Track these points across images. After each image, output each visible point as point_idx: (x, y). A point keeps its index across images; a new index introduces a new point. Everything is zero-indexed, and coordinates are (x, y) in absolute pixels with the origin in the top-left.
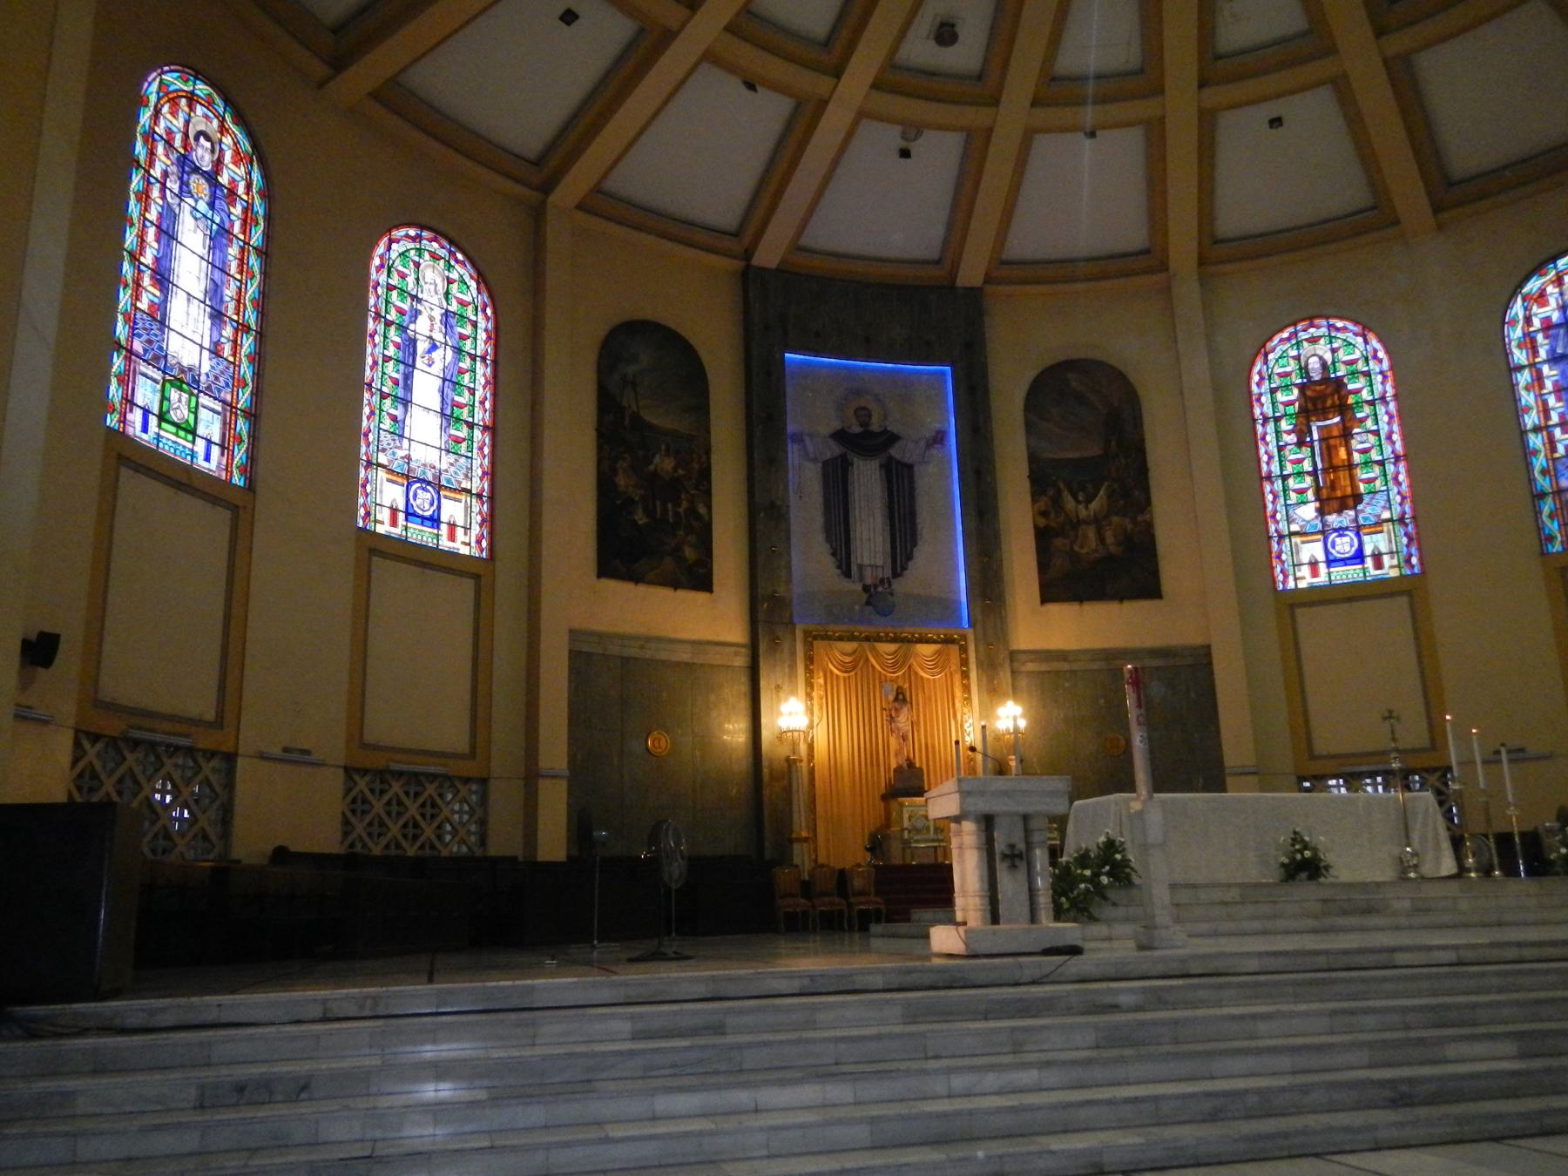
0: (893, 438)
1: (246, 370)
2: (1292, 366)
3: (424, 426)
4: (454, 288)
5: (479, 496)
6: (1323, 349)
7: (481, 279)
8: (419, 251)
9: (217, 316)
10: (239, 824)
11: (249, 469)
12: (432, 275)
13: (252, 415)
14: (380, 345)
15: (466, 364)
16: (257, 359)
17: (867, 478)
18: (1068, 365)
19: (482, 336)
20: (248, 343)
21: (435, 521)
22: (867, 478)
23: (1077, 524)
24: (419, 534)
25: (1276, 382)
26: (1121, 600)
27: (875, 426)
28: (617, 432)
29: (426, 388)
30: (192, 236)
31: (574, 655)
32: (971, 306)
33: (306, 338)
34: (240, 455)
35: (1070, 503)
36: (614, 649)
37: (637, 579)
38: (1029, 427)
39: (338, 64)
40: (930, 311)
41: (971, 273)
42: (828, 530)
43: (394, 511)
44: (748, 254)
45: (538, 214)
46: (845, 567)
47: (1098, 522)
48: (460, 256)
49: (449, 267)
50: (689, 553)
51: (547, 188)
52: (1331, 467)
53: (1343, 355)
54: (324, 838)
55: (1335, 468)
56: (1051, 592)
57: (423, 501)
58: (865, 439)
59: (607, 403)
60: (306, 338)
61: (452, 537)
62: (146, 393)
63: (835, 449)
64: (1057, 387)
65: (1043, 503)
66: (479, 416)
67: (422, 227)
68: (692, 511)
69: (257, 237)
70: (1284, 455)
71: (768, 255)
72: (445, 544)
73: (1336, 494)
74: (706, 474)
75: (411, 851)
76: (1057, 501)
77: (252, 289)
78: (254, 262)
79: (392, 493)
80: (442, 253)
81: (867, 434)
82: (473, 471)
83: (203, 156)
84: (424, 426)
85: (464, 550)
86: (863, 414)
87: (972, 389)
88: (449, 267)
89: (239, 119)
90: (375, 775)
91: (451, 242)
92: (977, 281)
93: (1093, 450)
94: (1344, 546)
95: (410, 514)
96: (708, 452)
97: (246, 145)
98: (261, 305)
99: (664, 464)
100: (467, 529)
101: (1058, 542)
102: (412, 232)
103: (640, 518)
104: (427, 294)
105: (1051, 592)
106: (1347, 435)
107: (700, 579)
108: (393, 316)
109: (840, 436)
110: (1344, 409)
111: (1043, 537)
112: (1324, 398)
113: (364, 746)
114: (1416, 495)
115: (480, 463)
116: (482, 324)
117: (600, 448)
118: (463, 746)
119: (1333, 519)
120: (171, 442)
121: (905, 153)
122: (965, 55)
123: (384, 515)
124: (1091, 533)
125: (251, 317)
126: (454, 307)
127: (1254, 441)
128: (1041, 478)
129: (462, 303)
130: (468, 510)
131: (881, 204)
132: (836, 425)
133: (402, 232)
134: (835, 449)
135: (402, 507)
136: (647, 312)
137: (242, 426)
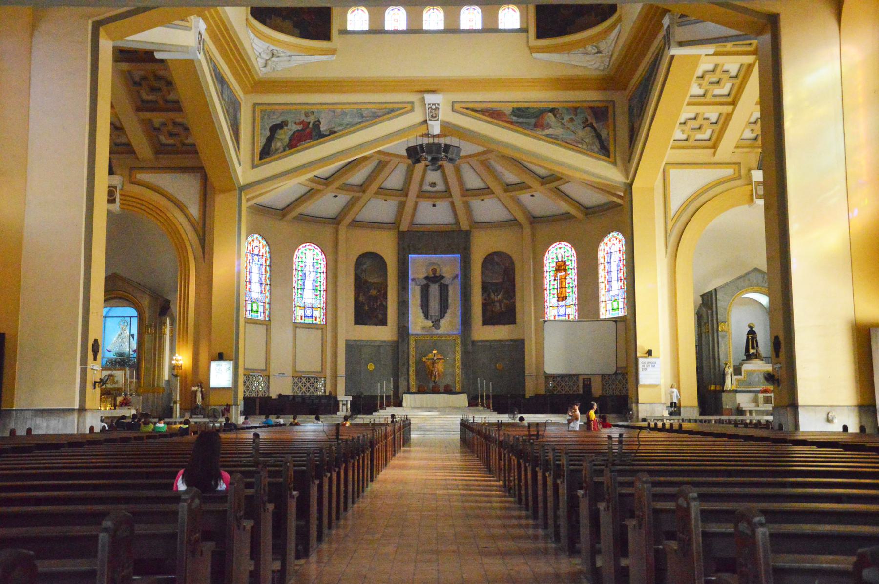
0: (443, 277)
1: (268, 294)
2: (555, 256)
3: (308, 294)
6: (562, 251)
7: (322, 251)
9: (261, 284)
10: (271, 390)
11: (269, 316)
12: (309, 254)
13: (269, 304)
14: (297, 276)
15: (319, 275)
16: (270, 291)
17: (434, 289)
18: (495, 253)
20: (268, 288)
21: (312, 317)
22: (434, 289)
23: (493, 302)
25: (551, 260)
26: (504, 324)
27: (437, 274)
28: (360, 285)
29: (309, 284)
30: (255, 269)
31: (347, 345)
32: (467, 235)
33: (280, 271)
34: (267, 313)
35: (492, 296)
36: (358, 343)
37: (366, 324)
38: (483, 273)
39: (284, 216)
40: (455, 239)
41: (465, 226)
42: (422, 306)
44: (398, 227)
45: (337, 231)
46: (427, 316)
47: (500, 302)
50: (380, 316)
51: (339, 224)
52: (561, 288)
53: (567, 254)
54: (288, 391)
55: (561, 288)
56: (485, 323)
57: (309, 313)
58: (434, 278)
59: (357, 278)
60: (280, 271)
62: (249, 308)
63: (425, 282)
64: (490, 260)
65: (486, 294)
66: (323, 288)
68: (382, 304)
69: (268, 263)
70: (550, 282)
71: (404, 227)
72: (314, 322)
73: (562, 298)
74: (386, 294)
75: (308, 394)
76: (489, 295)
77: (268, 275)
78: (268, 269)
79: (301, 312)
81: (435, 277)
82: (320, 302)
83: (256, 252)
84: (308, 294)
86: (434, 271)
87: (465, 262)
89: (263, 238)
90: (298, 377)
92: (468, 228)
93: (500, 280)
94: (562, 311)
96: (387, 286)
97: (264, 243)
98: (270, 279)
99: (373, 292)
101: (489, 308)
103: (366, 308)
104: (310, 259)
105: (485, 323)
106: (565, 278)
107: (384, 323)
108: (300, 269)
109: (427, 278)
110: (565, 270)
111: (485, 306)
112: (561, 267)
113: (296, 371)
114: (579, 299)
115: (323, 300)
117: (355, 290)
118: (319, 369)
119: (561, 303)
120: (254, 316)
121: (434, 206)
122: (440, 187)
124: (498, 304)
125: (268, 282)
126: (315, 261)
127: (543, 278)
128: (485, 288)
131: (434, 215)
132: (425, 275)
134: (425, 282)
136: (370, 249)
137: (267, 306)
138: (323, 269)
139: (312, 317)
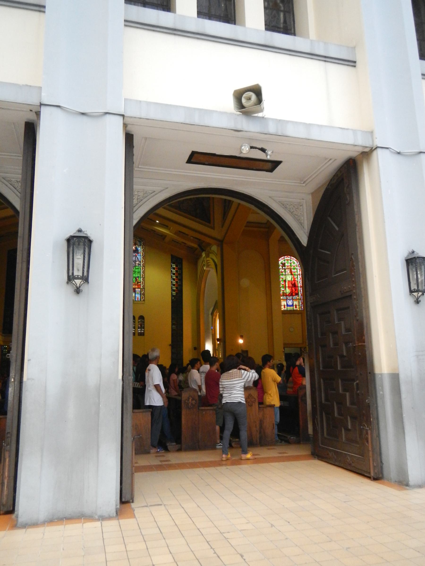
4: (292, 264)
5: (301, 299)
8: (284, 261)
19: (298, 270)
21: (293, 305)
24: (289, 308)
43: (284, 306)
48: (293, 258)
49: (291, 261)
61: (296, 307)
67: (284, 256)
72: (295, 309)
80: (289, 259)
85: (298, 309)
88: (291, 261)
91: (291, 256)
95: (287, 305)
100: (299, 305)
102: (282, 258)
116: (298, 268)
123: (283, 307)
129: (294, 266)
130: (299, 302)
133: (281, 259)
135: (286, 304)
138: (299, 272)
139: (293, 305)
